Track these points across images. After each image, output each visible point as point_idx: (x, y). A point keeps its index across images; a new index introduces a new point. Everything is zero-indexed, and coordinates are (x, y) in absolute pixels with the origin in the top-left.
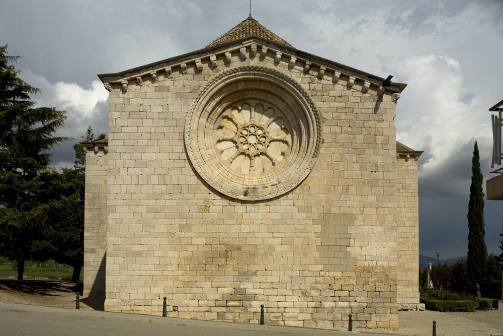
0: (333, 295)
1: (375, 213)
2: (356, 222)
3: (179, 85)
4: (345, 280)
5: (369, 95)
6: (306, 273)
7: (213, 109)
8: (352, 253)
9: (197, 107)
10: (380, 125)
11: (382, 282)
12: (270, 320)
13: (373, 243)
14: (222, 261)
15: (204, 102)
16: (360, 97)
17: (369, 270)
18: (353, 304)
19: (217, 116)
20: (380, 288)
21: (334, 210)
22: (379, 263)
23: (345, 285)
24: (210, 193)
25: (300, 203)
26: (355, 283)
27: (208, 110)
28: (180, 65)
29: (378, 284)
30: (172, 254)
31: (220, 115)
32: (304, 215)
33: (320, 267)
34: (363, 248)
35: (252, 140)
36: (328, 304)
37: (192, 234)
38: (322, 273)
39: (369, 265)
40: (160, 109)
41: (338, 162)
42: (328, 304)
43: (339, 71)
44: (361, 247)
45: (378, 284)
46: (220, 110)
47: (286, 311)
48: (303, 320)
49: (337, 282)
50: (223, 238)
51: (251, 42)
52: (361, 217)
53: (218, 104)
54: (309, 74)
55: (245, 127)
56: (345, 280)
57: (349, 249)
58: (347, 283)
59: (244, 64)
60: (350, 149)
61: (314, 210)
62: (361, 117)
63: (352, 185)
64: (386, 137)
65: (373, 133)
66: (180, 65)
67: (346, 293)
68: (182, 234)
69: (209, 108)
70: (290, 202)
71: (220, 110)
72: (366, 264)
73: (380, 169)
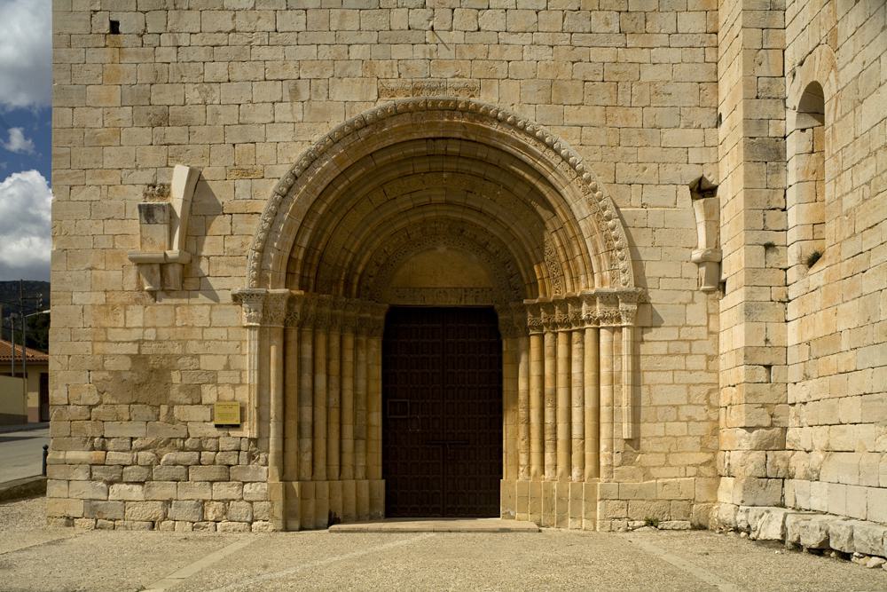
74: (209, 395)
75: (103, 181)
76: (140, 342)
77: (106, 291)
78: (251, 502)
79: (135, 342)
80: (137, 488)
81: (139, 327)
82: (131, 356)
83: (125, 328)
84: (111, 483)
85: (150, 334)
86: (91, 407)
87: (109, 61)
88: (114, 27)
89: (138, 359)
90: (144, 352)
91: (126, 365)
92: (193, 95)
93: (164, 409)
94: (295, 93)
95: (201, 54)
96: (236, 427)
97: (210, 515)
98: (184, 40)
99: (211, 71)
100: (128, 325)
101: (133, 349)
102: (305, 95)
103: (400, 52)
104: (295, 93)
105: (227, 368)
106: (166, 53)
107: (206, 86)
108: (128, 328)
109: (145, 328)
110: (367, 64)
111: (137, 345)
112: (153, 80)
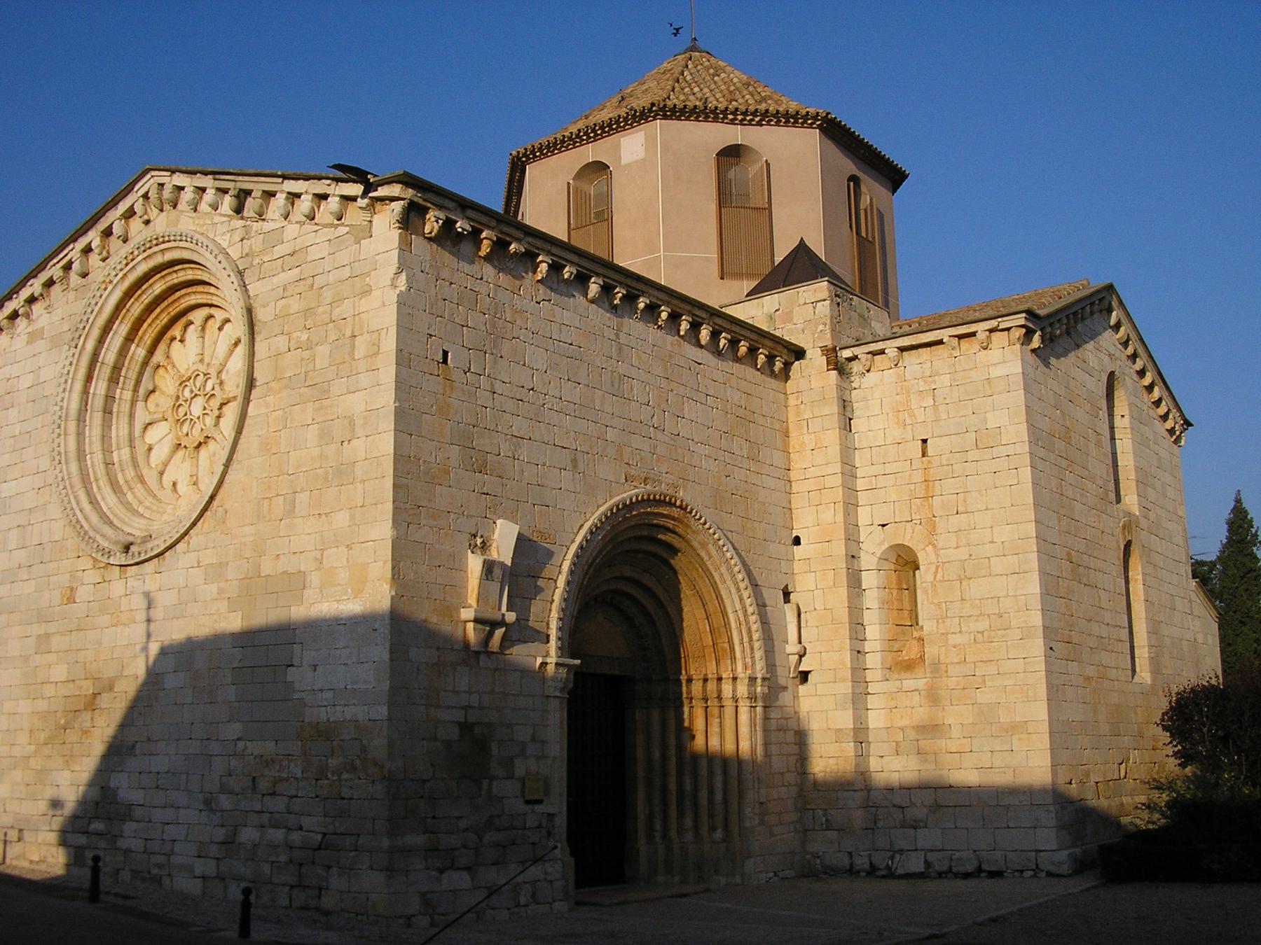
0: (258, 807)
1: (345, 562)
2: (307, 592)
3: (57, 319)
4: (281, 765)
5: (347, 229)
6: (214, 747)
7: (123, 352)
8: (297, 686)
9: (75, 362)
10: (365, 304)
11: (354, 769)
12: (149, 873)
13: (338, 652)
14: (86, 716)
15: (90, 345)
16: (329, 240)
17: (325, 732)
18: (296, 837)
19: (137, 369)
20: (351, 788)
21: (268, 567)
22: (350, 713)
23: (281, 780)
24: (79, 557)
25: (209, 558)
26: (299, 775)
27: (107, 361)
28: (52, 277)
29: (345, 776)
30: (25, 707)
31: (145, 363)
32: (213, 589)
33: (235, 730)
34: (319, 669)
35: (197, 408)
36: (248, 835)
37: (51, 658)
38: (241, 744)
39: (328, 720)
40: (27, 381)
41: (280, 431)
42: (248, 835)
43: (282, 191)
44: (315, 666)
45: (345, 776)
46: (138, 352)
47: (177, 849)
48: (203, 877)
49: (266, 772)
50: (91, 663)
51: (150, 179)
52: (314, 579)
53: (129, 339)
54: (242, 218)
55: (184, 381)
56: (281, 765)
57: (292, 674)
58: (284, 775)
59: (148, 233)
60: (303, 390)
61: (231, 573)
62: (328, 295)
63: (302, 490)
64: (376, 335)
65: (348, 333)
66: (52, 277)
67: (279, 804)
68: (38, 656)
69: (109, 355)
70: (193, 555)
71: (138, 352)
72: (323, 715)
73: (360, 431)
74: (520, 770)
75: (435, 523)
76: (466, 708)
77: (438, 649)
78: (551, 882)
79: (462, 708)
80: (465, 876)
81: (465, 692)
82: (459, 723)
83: (453, 691)
84: (441, 871)
85: (474, 701)
86: (424, 782)
87: (442, 392)
88: (445, 354)
89: (466, 727)
90: (470, 720)
91: (455, 733)
92: (505, 448)
93: (485, 784)
94: (574, 462)
95: (510, 406)
96: (540, 802)
97: (523, 901)
98: (498, 387)
99: (520, 426)
100: (457, 689)
101: (459, 716)
102: (581, 467)
103: (637, 442)
104: (574, 462)
105: (533, 739)
106: (484, 397)
107: (515, 439)
108: (457, 692)
109: (471, 693)
110: (620, 450)
111: (463, 712)
112: (473, 421)
